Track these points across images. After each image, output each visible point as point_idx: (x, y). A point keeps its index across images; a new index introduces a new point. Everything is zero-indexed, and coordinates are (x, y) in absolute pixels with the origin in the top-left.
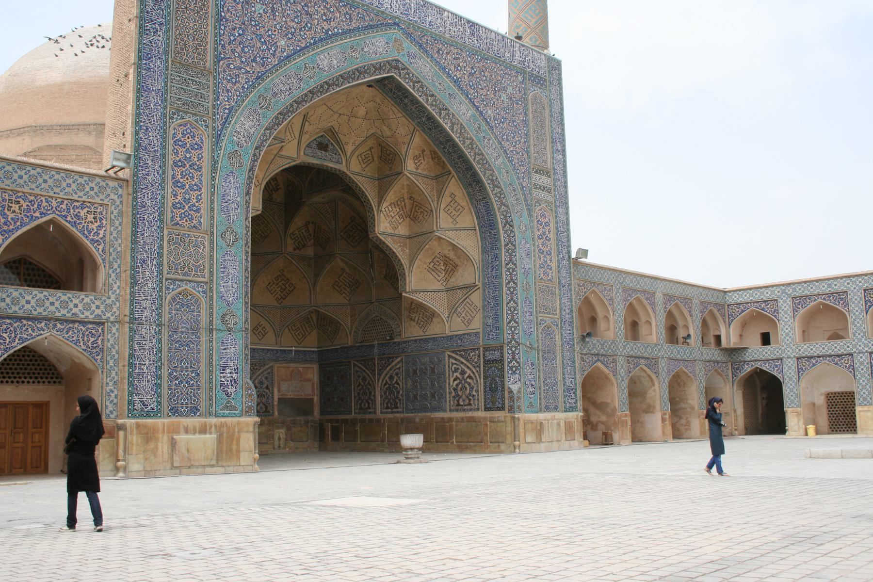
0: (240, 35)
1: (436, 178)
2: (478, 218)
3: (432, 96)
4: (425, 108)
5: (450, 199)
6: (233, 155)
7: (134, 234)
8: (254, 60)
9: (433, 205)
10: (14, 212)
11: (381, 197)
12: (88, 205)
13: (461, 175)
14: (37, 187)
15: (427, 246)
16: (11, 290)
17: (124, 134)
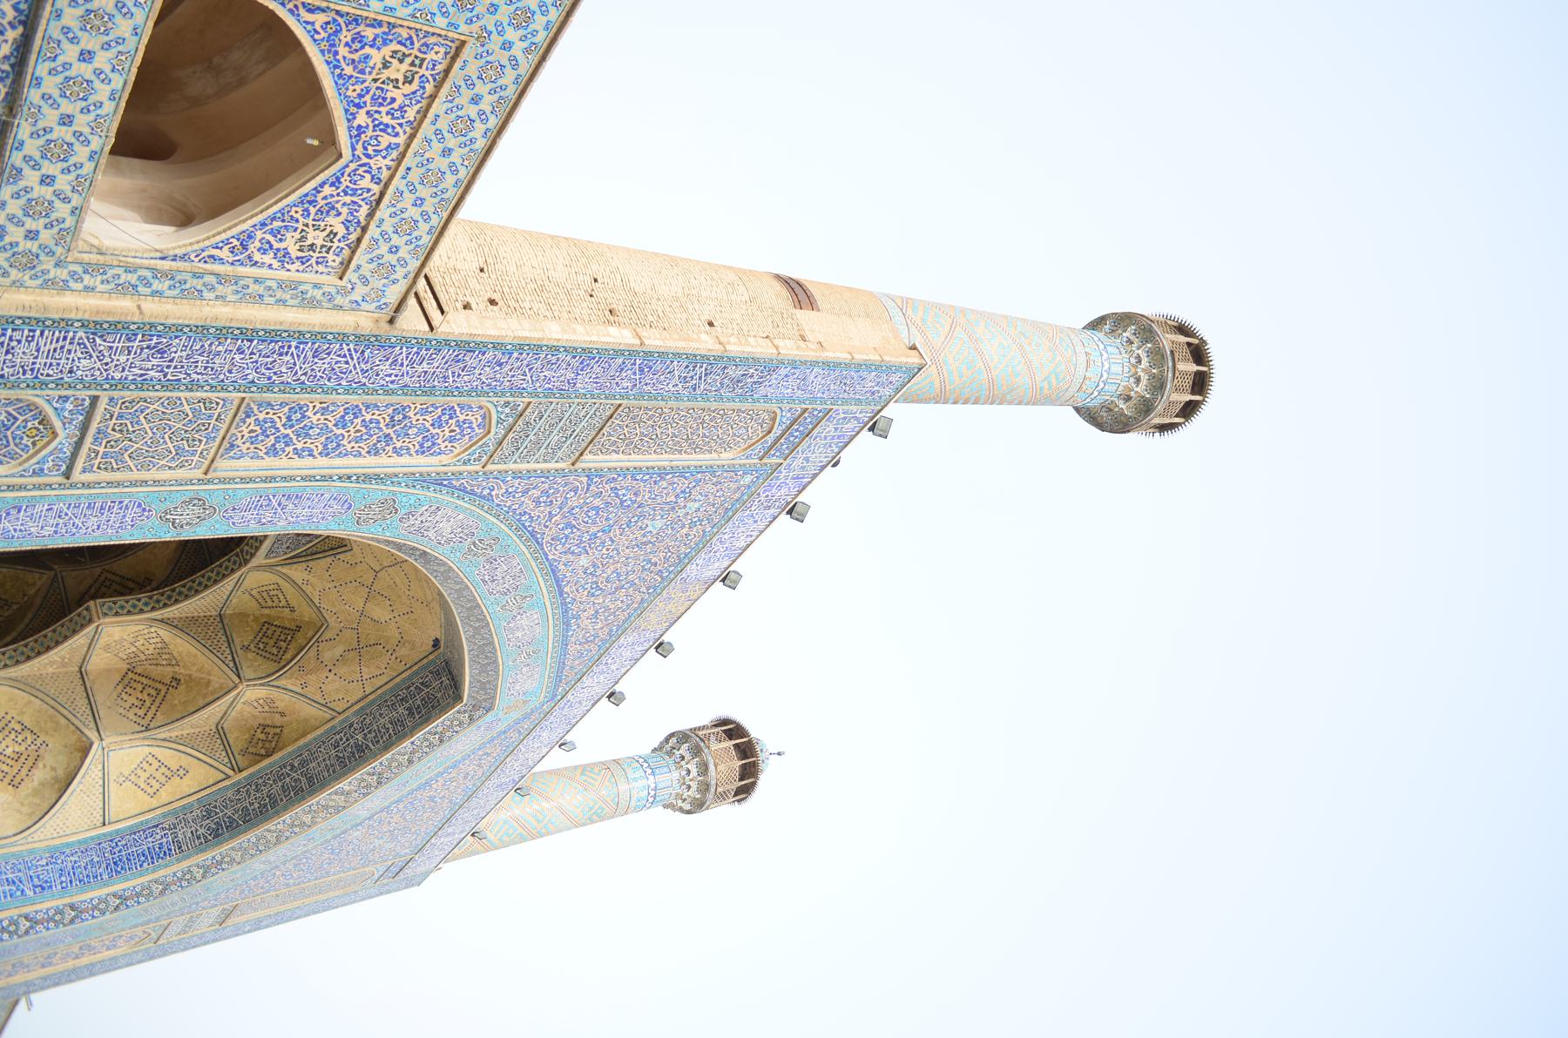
0: (622, 502)
1: (220, 732)
2: (133, 831)
3: (410, 762)
4: (386, 748)
5: (174, 768)
6: (390, 506)
7: (247, 334)
8: (568, 525)
9: (163, 733)
10: (386, 65)
11: (183, 626)
12: (353, 237)
13: (230, 794)
14: (438, 132)
15: (63, 721)
16: (139, 16)
17: (492, 302)
